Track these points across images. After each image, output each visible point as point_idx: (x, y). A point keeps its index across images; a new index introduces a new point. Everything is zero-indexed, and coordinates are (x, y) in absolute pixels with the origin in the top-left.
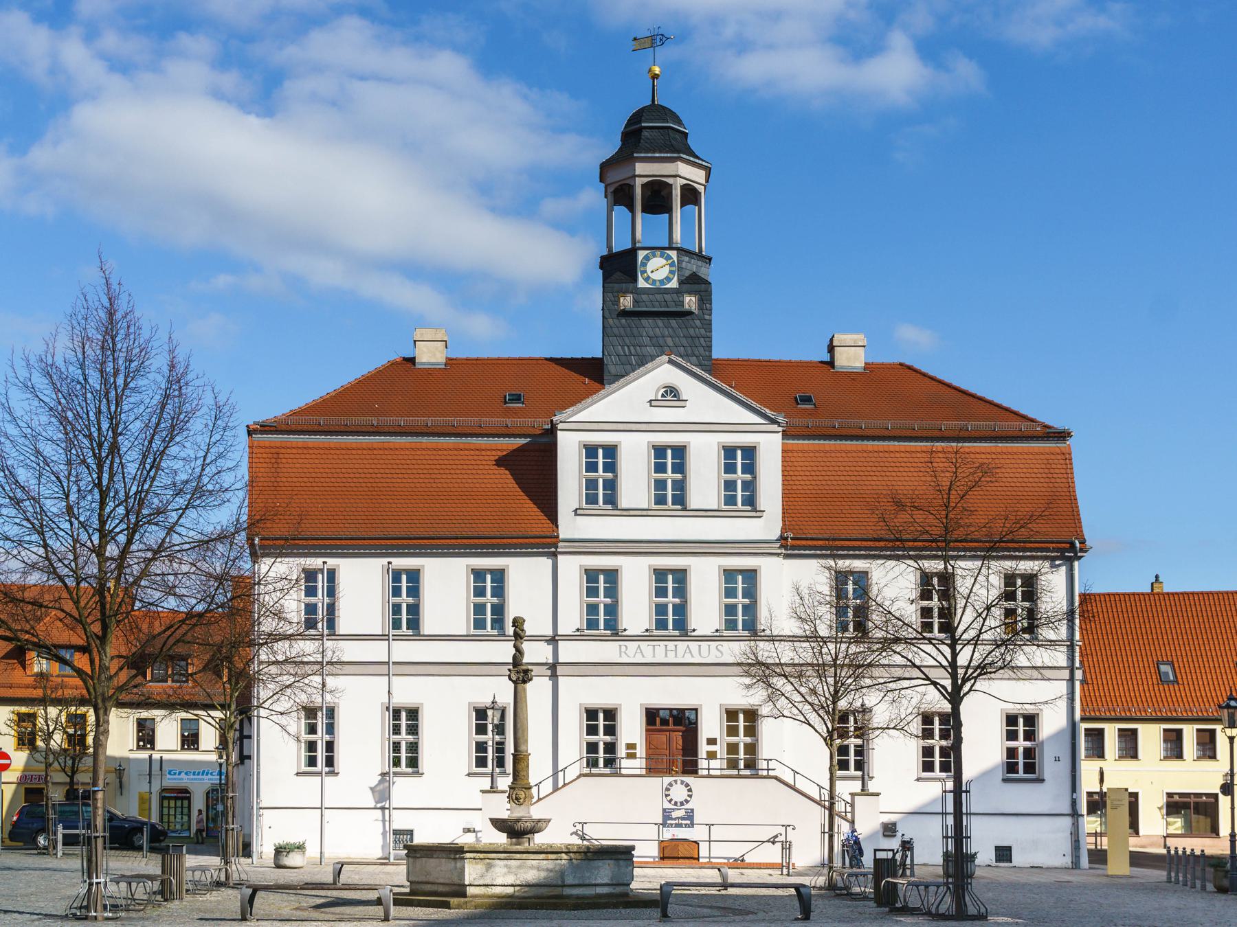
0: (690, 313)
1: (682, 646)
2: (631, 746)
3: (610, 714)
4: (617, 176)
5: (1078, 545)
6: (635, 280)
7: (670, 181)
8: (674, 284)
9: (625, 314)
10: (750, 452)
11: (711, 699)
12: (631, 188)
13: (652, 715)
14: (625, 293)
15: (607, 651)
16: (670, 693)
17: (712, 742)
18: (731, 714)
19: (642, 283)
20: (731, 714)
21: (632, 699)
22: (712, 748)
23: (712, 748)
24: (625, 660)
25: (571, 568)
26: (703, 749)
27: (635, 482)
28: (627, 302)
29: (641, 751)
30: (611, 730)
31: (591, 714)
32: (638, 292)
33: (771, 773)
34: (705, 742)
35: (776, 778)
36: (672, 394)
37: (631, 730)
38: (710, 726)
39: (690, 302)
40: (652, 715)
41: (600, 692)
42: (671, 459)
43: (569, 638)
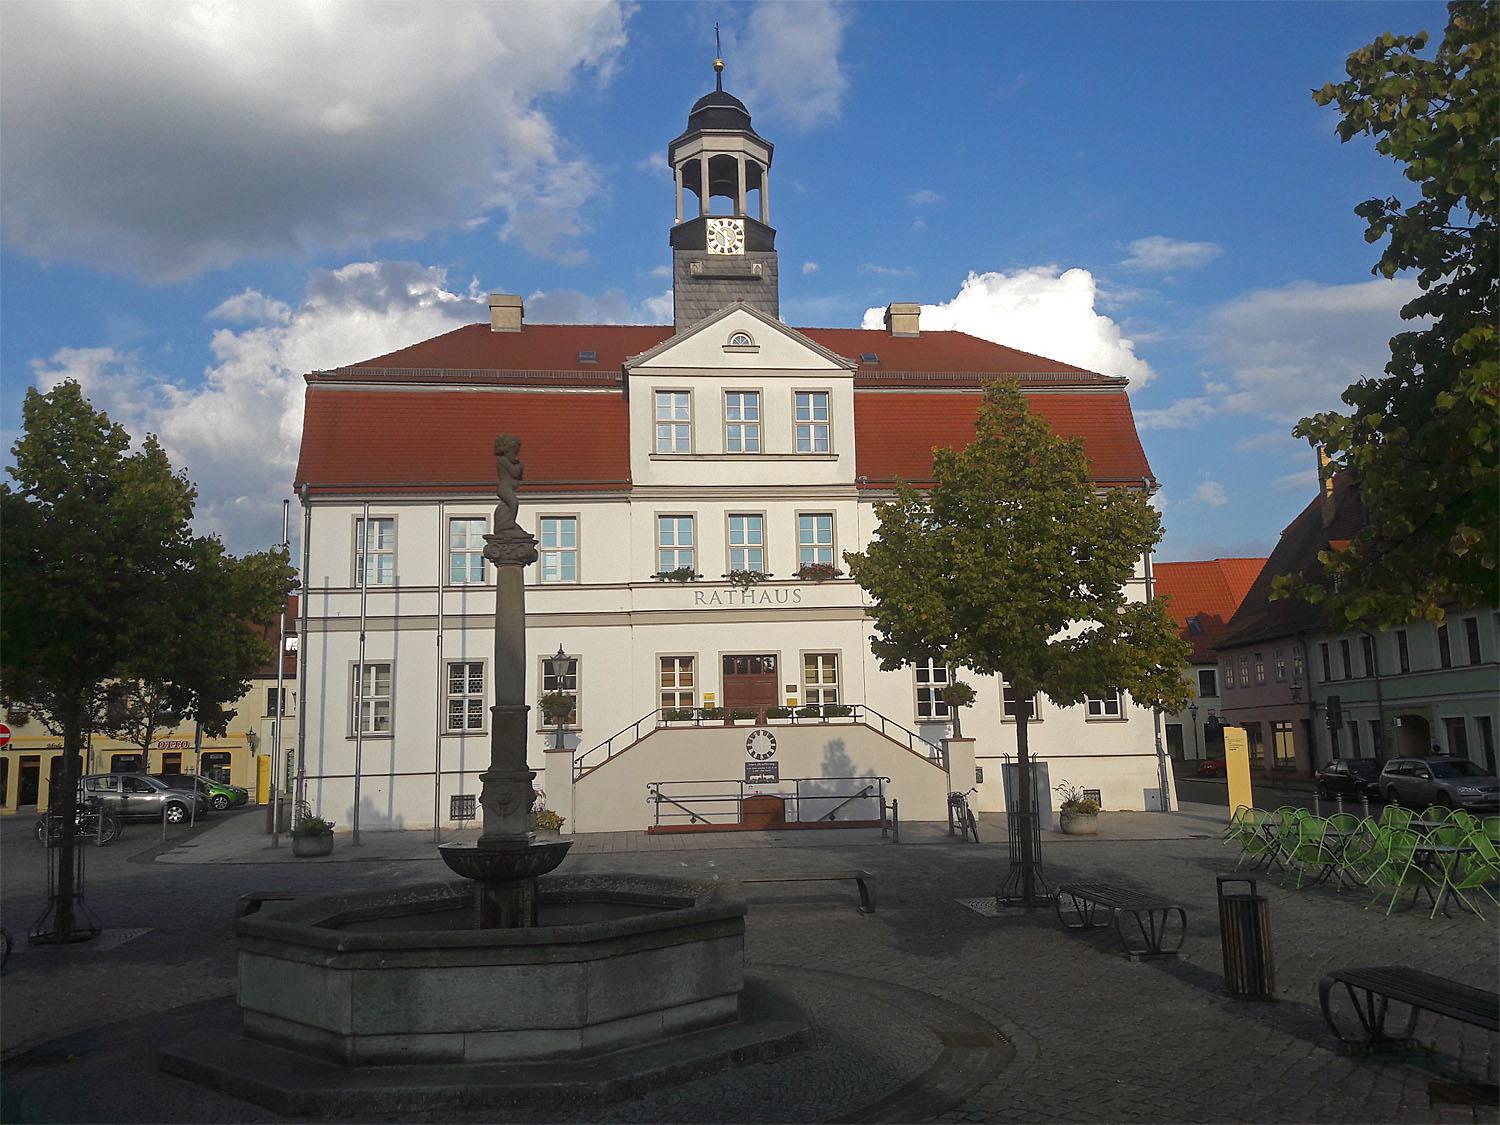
0: (757, 278)
1: (759, 590)
3: (687, 661)
4: (682, 153)
5: (1148, 483)
6: (704, 248)
7: (736, 155)
8: (741, 251)
9: (697, 278)
11: (788, 645)
12: (698, 163)
13: (729, 662)
16: (748, 640)
17: (792, 689)
18: (810, 659)
19: (711, 251)
20: (810, 659)
21: (710, 648)
23: (792, 695)
25: (644, 512)
26: (784, 699)
28: (698, 268)
30: (687, 680)
31: (667, 662)
32: (708, 258)
33: (858, 720)
35: (865, 724)
38: (790, 672)
39: (756, 268)
40: (729, 662)
41: (676, 640)
42: (744, 400)
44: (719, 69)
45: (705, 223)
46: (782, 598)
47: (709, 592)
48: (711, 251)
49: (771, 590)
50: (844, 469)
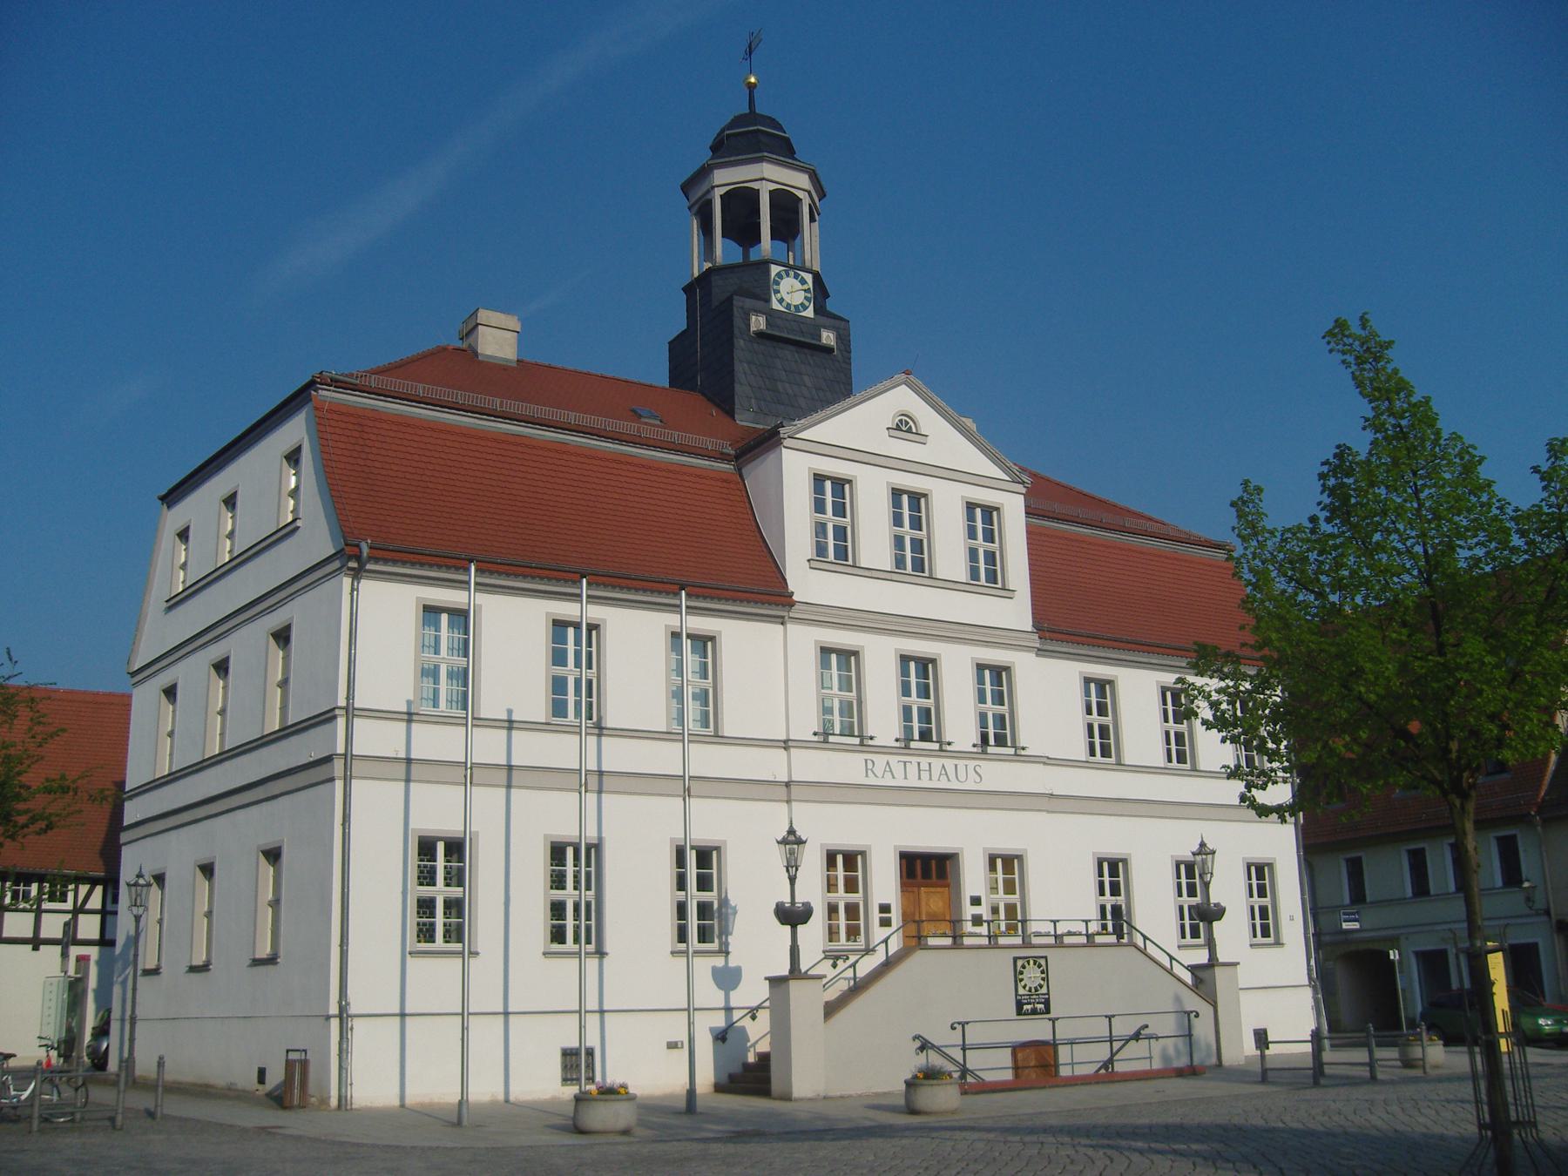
1: (937, 763)
2: (885, 908)
6: (768, 301)
8: (809, 313)
10: (989, 512)
11: (968, 837)
14: (758, 312)
15: (845, 766)
17: (976, 901)
21: (885, 836)
22: (976, 910)
23: (976, 910)
24: (872, 781)
25: (804, 639)
26: (969, 911)
27: (874, 536)
29: (895, 916)
32: (771, 315)
34: (968, 901)
36: (904, 427)
37: (884, 883)
38: (974, 878)
39: (828, 338)
42: (910, 506)
43: (804, 745)
44: (751, 87)
45: (768, 272)
46: (962, 776)
47: (880, 760)
48: (776, 305)
49: (949, 764)
50: (1016, 612)
